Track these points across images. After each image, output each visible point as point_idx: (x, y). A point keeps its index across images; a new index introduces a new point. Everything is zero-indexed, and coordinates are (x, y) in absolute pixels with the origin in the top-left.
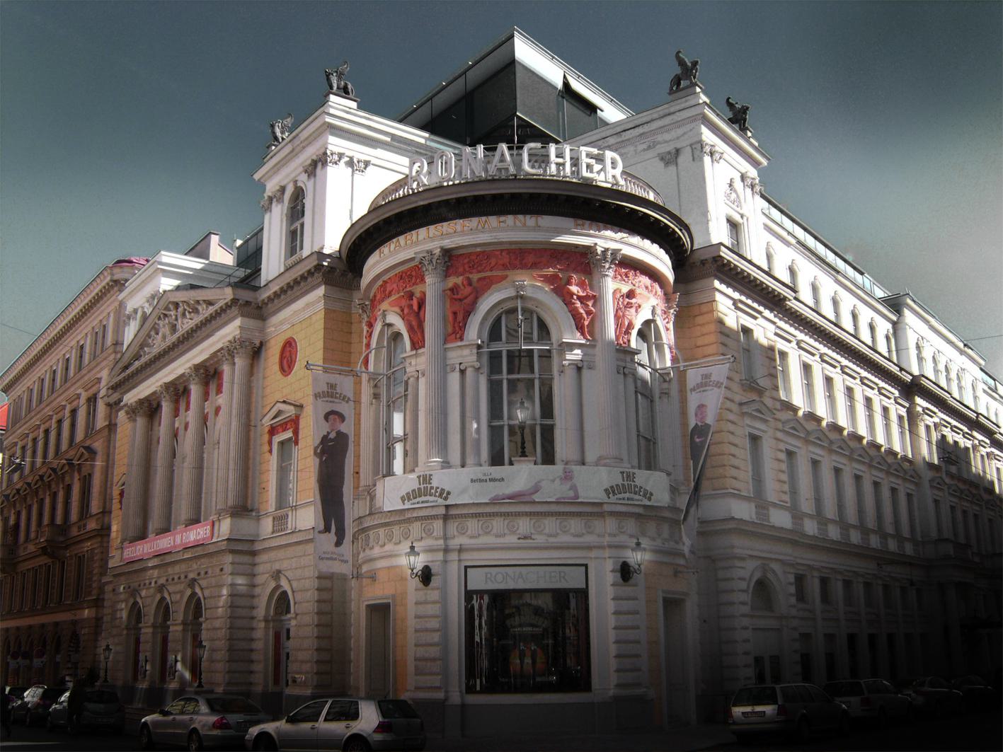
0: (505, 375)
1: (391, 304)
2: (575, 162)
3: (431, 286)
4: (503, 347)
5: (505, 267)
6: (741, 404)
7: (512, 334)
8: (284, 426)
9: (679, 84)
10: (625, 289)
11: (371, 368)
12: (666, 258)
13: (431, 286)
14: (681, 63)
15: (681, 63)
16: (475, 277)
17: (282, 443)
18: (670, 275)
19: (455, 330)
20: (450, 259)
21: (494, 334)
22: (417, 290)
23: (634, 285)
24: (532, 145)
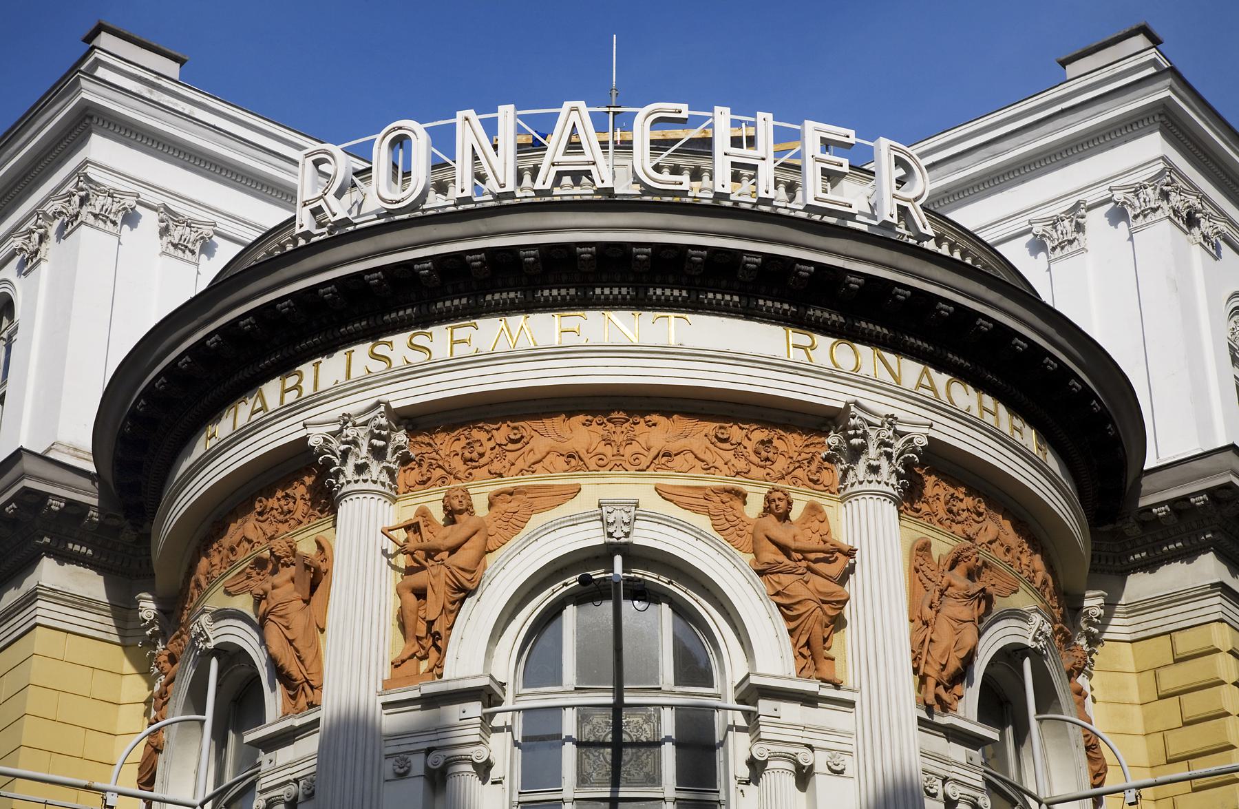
2: (790, 169)
10: (942, 547)
23: (970, 539)
24: (667, 108)
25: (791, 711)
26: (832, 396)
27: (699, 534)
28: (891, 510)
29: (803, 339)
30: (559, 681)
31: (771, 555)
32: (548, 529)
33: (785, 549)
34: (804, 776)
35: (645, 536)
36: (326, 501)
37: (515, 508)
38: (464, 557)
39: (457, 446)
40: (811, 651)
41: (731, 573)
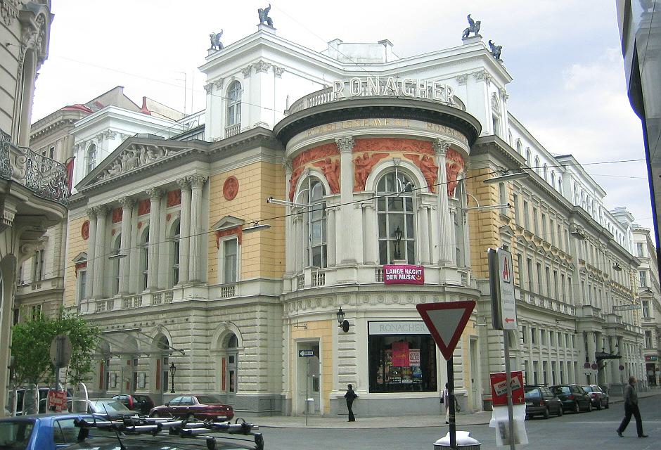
0: (387, 211)
1: (315, 165)
3: (346, 159)
4: (386, 193)
5: (388, 148)
6: (500, 228)
7: (393, 188)
8: (230, 231)
9: (468, 34)
10: (451, 163)
11: (296, 201)
12: (464, 139)
13: (346, 159)
14: (471, 22)
15: (471, 22)
16: (370, 153)
17: (226, 243)
18: (467, 149)
19: (360, 182)
20: (359, 143)
21: (381, 187)
22: (333, 159)
25: (427, 199)
26: (434, 136)
27: (411, 164)
28: (444, 158)
29: (430, 124)
30: (384, 191)
31: (424, 168)
32: (385, 162)
33: (426, 167)
34: (429, 209)
35: (402, 164)
36: (338, 152)
37: (377, 158)
38: (369, 167)
39: (365, 143)
40: (430, 187)
41: (417, 172)
